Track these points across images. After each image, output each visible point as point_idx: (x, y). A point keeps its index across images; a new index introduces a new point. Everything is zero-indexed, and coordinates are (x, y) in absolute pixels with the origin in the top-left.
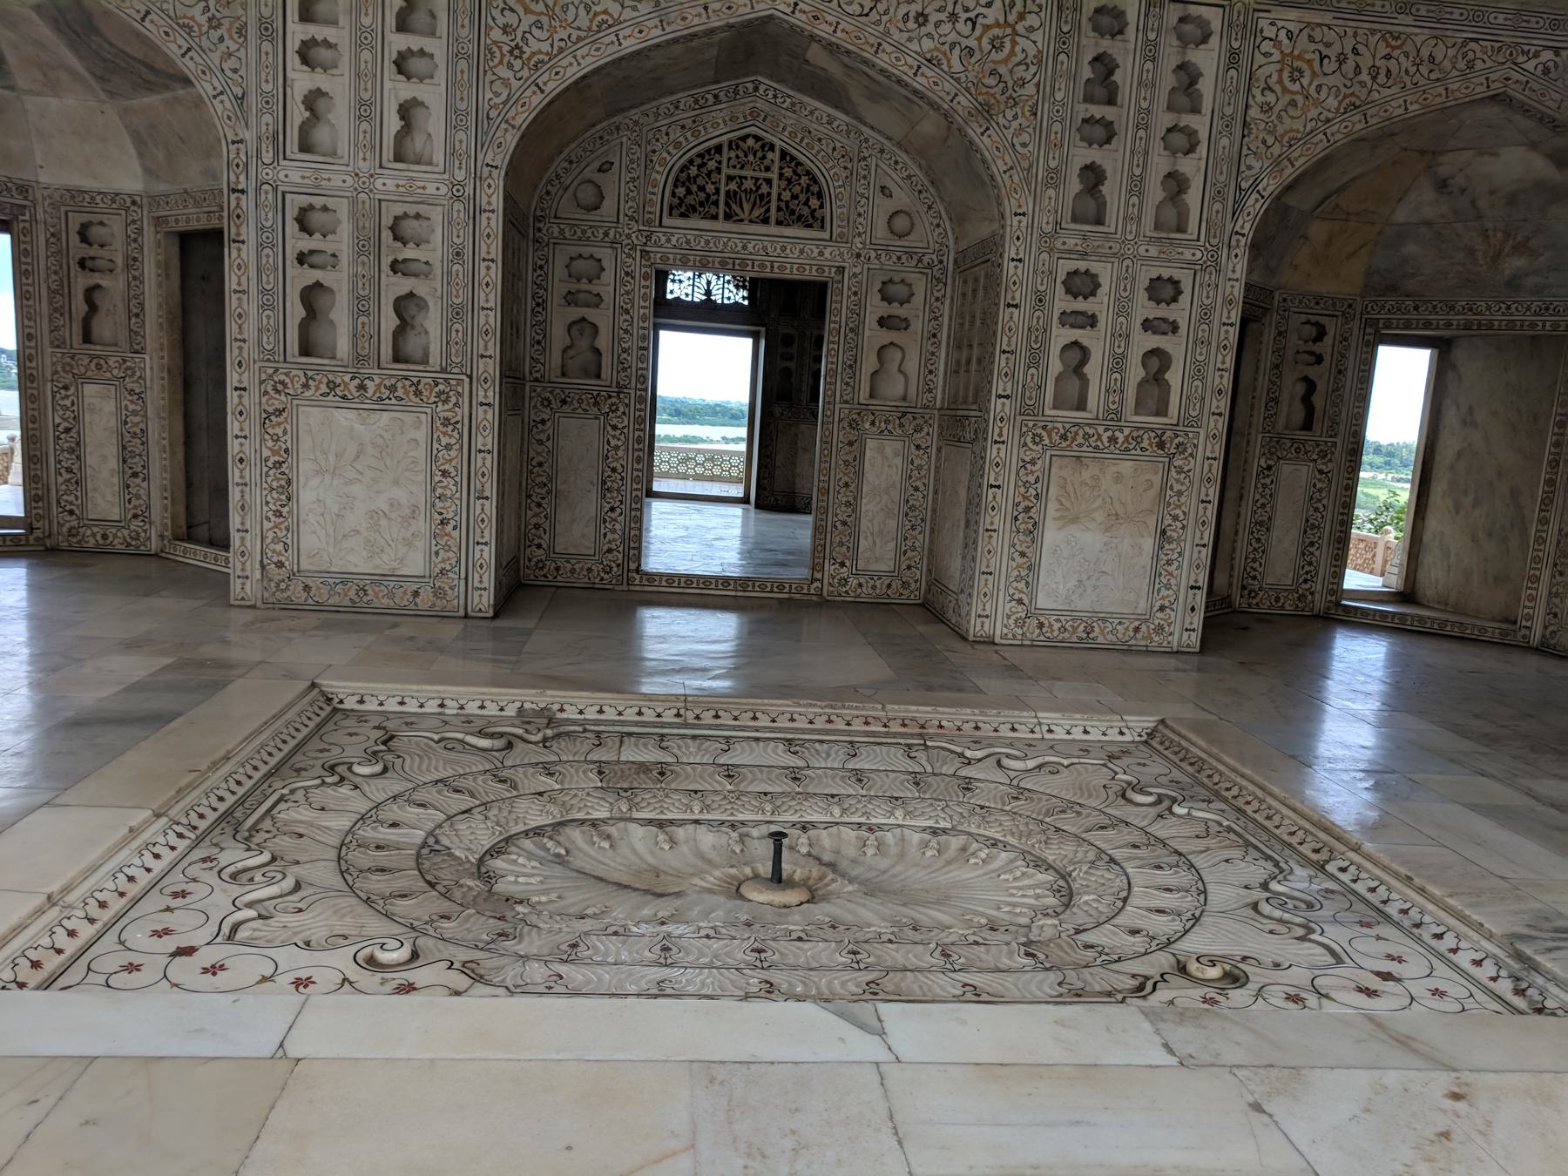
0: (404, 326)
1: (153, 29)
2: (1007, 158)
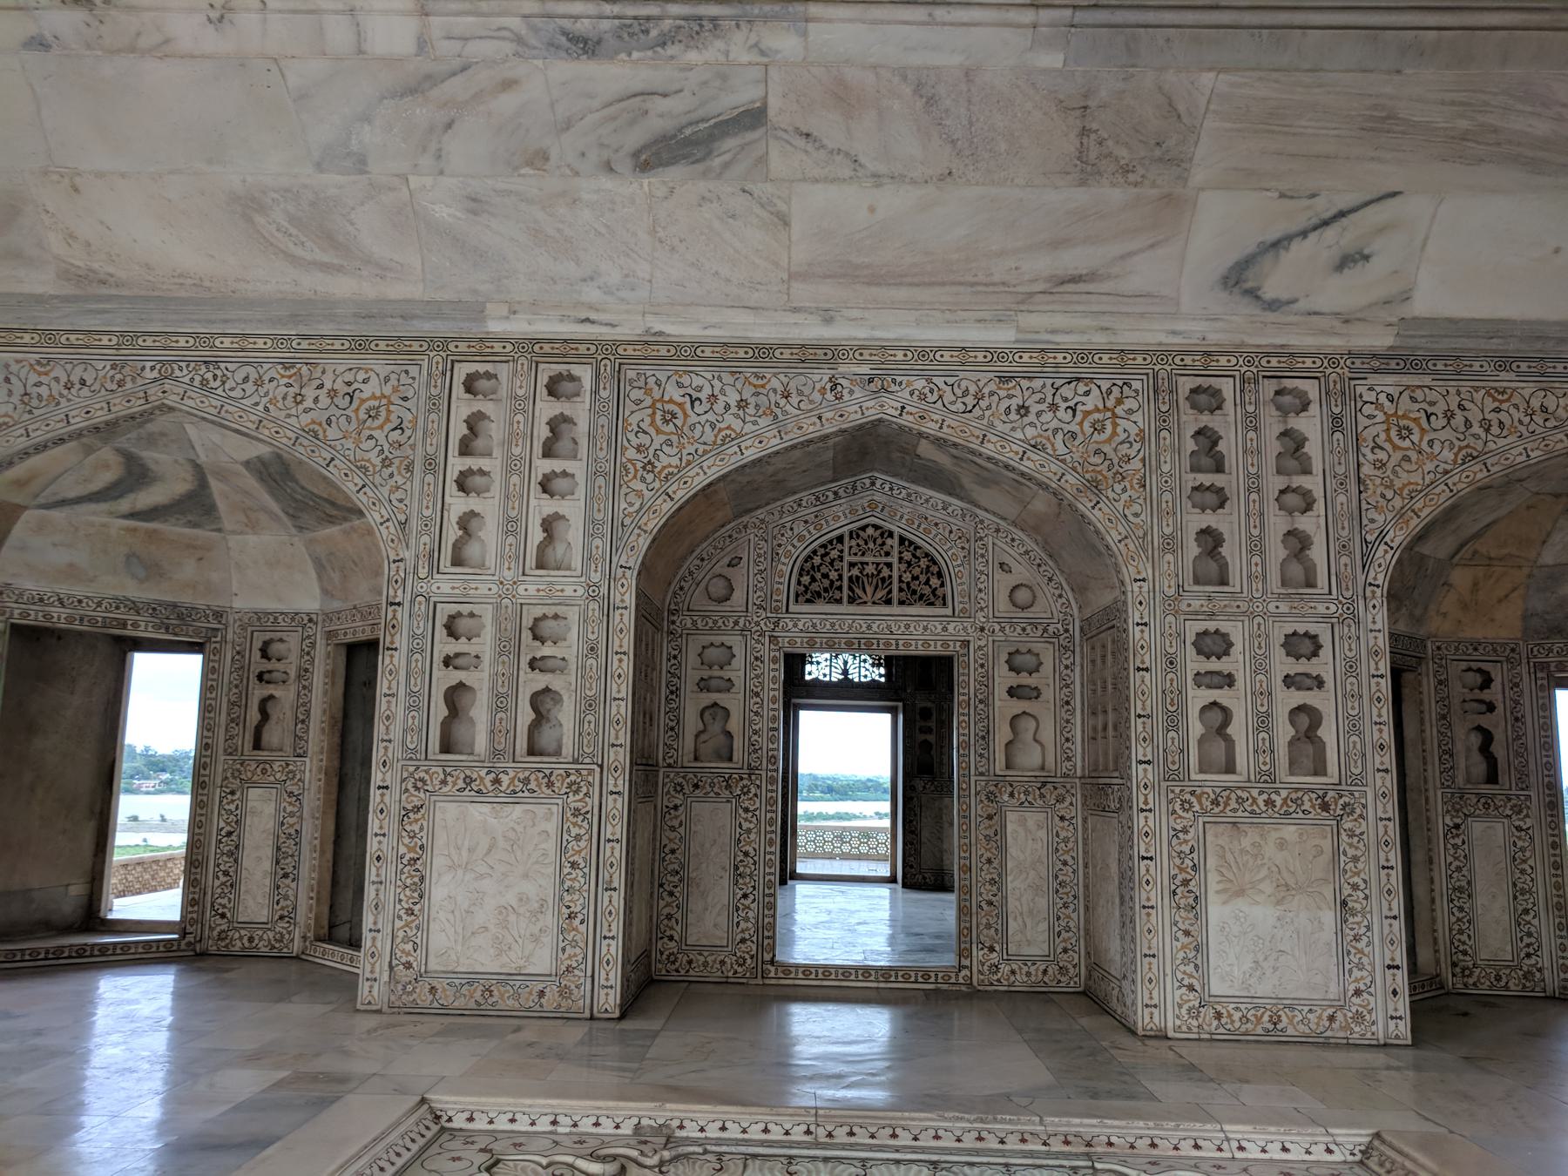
0: (540, 718)
1: (334, 473)
2: (1120, 528)
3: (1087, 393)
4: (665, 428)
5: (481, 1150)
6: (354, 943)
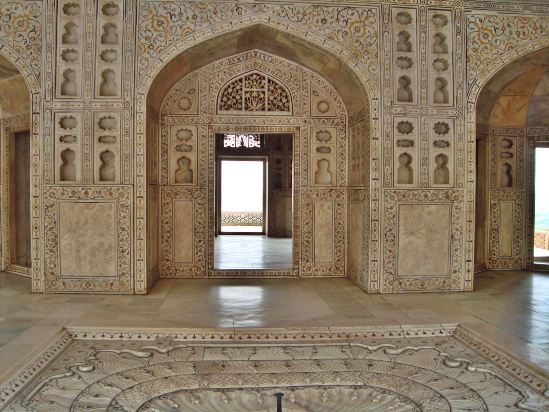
1: (4, 52)
2: (367, 75)
3: (352, 14)
4: (158, 28)
5: (91, 348)
6: (28, 265)
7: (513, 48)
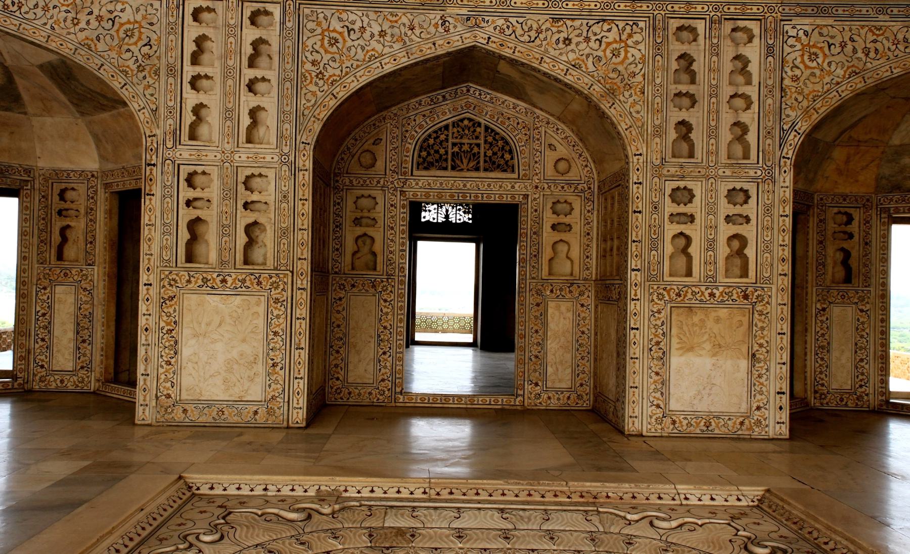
0: (251, 243)
1: (104, 74)
2: (627, 120)
3: (609, 30)
5: (219, 507)
6: (133, 383)
7: (857, 74)
